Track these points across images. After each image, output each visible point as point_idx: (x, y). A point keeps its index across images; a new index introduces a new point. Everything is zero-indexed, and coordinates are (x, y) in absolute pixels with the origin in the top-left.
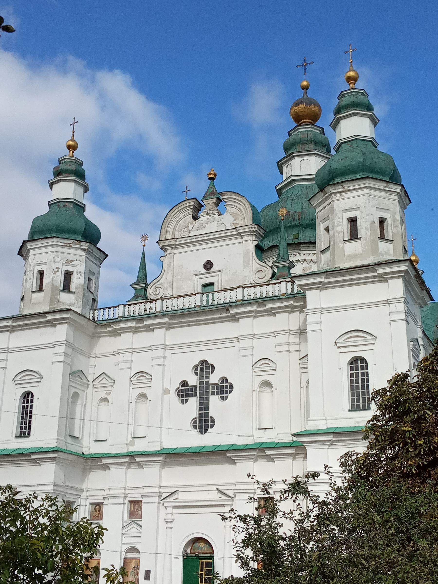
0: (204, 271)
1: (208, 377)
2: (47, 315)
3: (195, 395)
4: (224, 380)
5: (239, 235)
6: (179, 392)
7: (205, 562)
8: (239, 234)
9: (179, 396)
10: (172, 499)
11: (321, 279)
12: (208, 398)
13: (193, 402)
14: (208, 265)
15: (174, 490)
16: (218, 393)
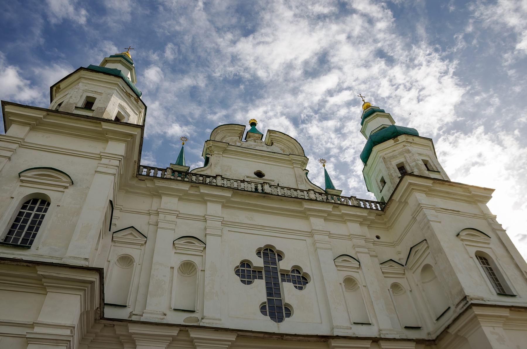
1: (275, 264)
4: (297, 269)
12: (277, 285)
13: (260, 285)
16: (289, 281)
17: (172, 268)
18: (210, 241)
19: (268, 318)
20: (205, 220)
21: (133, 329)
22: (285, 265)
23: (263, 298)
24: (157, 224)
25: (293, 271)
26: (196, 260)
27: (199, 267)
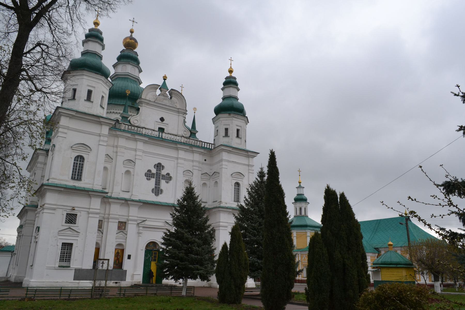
0: (160, 121)
1: (160, 171)
2: (100, 118)
3: (154, 177)
4: (168, 174)
5: (178, 112)
6: (146, 174)
7: (154, 253)
8: (179, 112)
9: (146, 176)
10: (143, 223)
11: (231, 149)
12: (159, 181)
13: (153, 180)
14: (162, 119)
15: (145, 219)
16: (164, 179)
17: (122, 174)
18: (137, 162)
19: (154, 194)
20: (136, 151)
21: (110, 200)
22: (164, 172)
23: (153, 186)
24: (117, 152)
25: (166, 175)
26: (131, 170)
27: (132, 174)
